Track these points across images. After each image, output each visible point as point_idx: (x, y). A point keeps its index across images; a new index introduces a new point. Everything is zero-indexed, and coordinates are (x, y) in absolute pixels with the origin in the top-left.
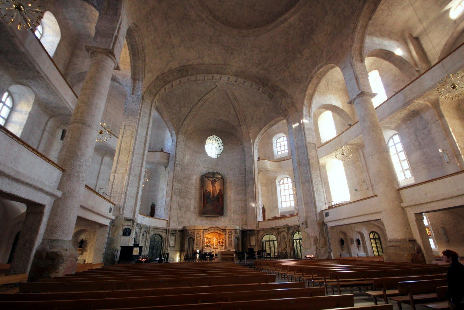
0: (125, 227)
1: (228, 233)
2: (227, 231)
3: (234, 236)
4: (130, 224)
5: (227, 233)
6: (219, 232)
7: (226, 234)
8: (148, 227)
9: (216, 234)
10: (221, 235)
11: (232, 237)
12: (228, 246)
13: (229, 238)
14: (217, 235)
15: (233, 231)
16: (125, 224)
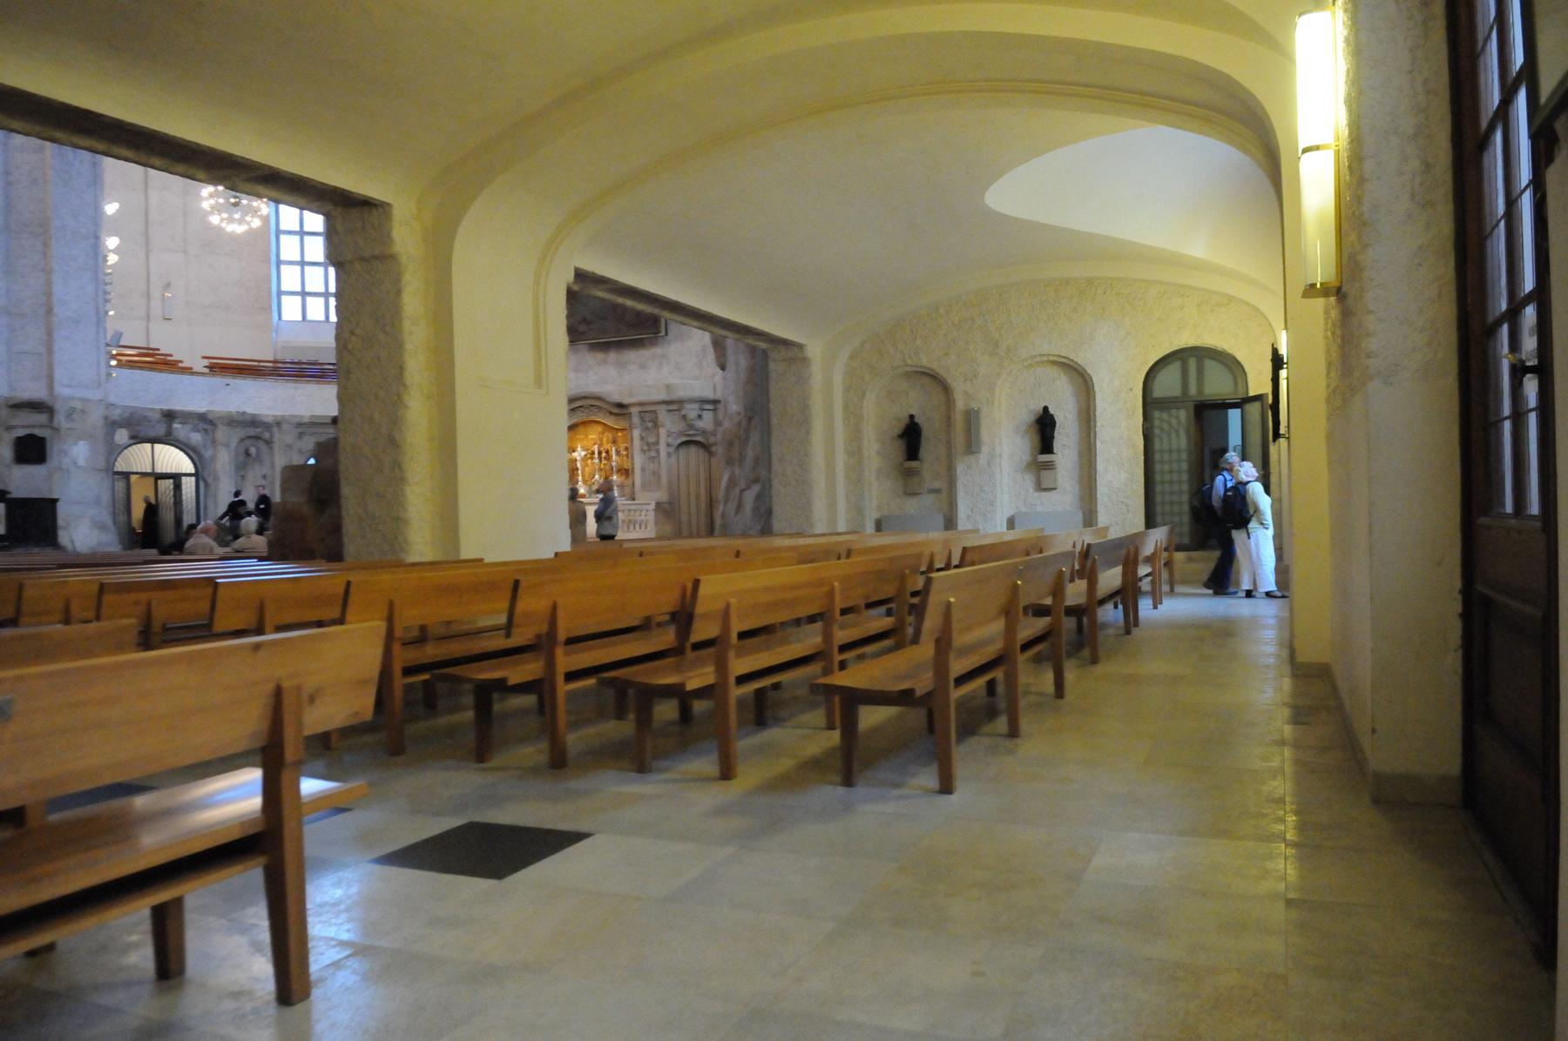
0: (21, 433)
1: (642, 419)
2: (634, 410)
3: (669, 434)
4: (42, 418)
5: (636, 420)
6: (610, 421)
7: (631, 428)
8: (269, 420)
9: (600, 428)
10: (620, 434)
11: (657, 443)
12: (643, 485)
13: (646, 448)
14: (603, 433)
15: (664, 407)
16: (15, 422)
